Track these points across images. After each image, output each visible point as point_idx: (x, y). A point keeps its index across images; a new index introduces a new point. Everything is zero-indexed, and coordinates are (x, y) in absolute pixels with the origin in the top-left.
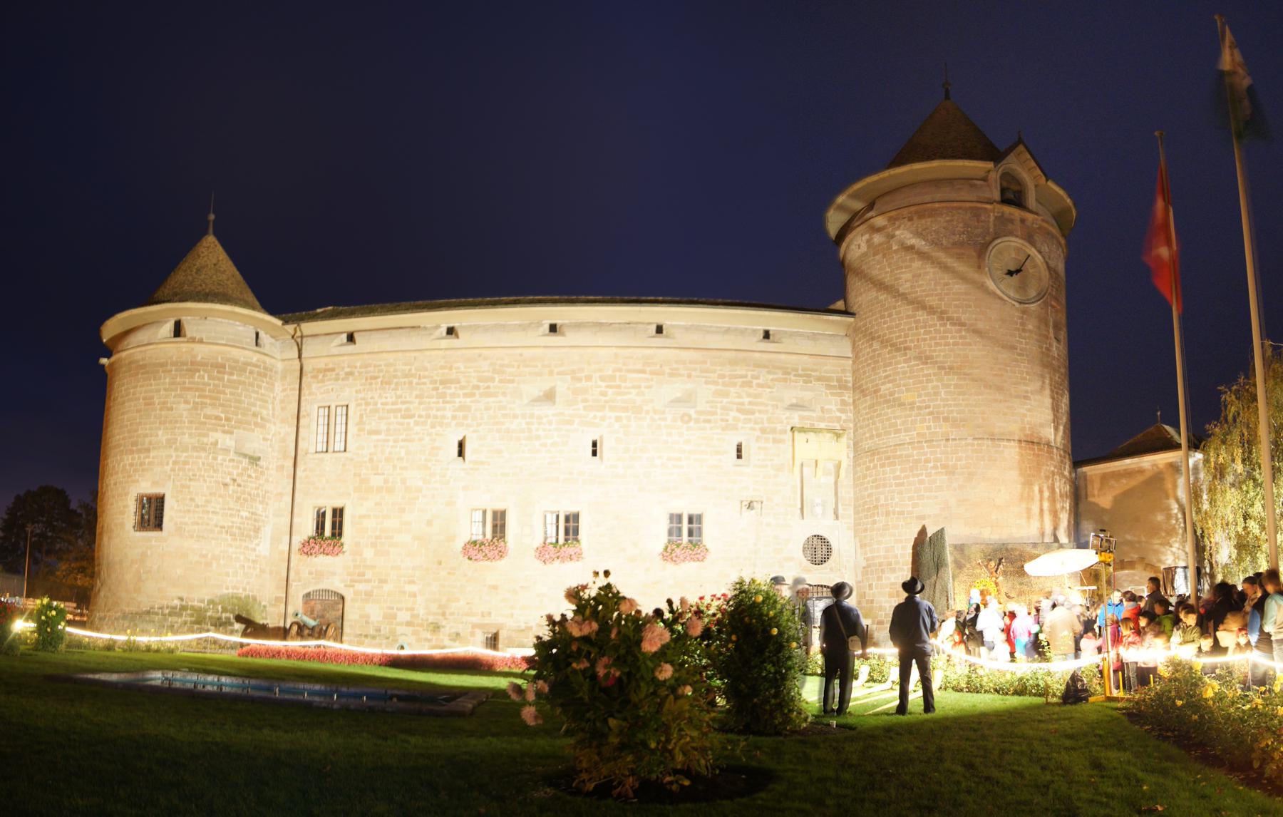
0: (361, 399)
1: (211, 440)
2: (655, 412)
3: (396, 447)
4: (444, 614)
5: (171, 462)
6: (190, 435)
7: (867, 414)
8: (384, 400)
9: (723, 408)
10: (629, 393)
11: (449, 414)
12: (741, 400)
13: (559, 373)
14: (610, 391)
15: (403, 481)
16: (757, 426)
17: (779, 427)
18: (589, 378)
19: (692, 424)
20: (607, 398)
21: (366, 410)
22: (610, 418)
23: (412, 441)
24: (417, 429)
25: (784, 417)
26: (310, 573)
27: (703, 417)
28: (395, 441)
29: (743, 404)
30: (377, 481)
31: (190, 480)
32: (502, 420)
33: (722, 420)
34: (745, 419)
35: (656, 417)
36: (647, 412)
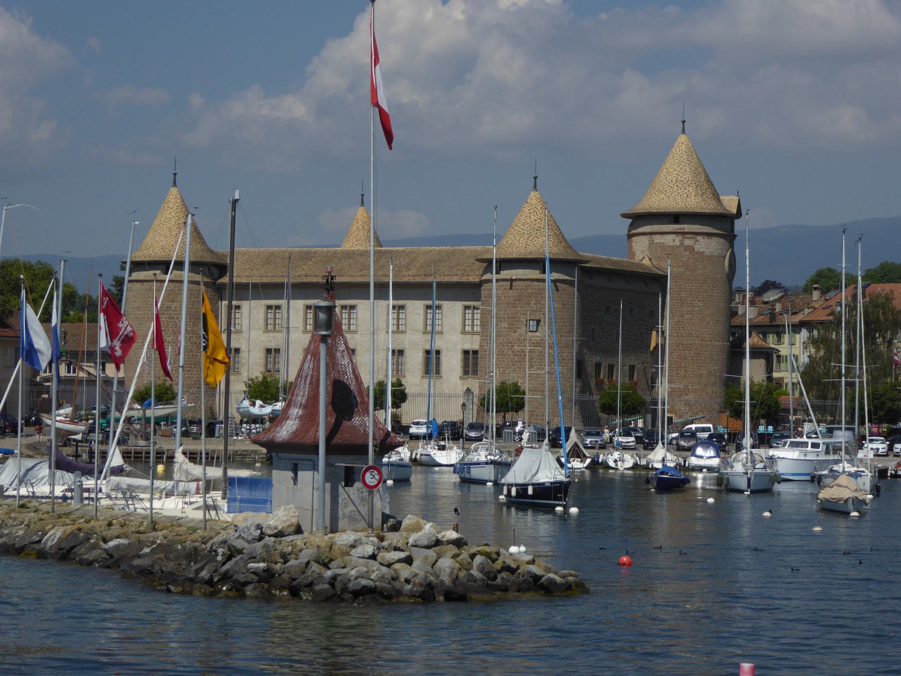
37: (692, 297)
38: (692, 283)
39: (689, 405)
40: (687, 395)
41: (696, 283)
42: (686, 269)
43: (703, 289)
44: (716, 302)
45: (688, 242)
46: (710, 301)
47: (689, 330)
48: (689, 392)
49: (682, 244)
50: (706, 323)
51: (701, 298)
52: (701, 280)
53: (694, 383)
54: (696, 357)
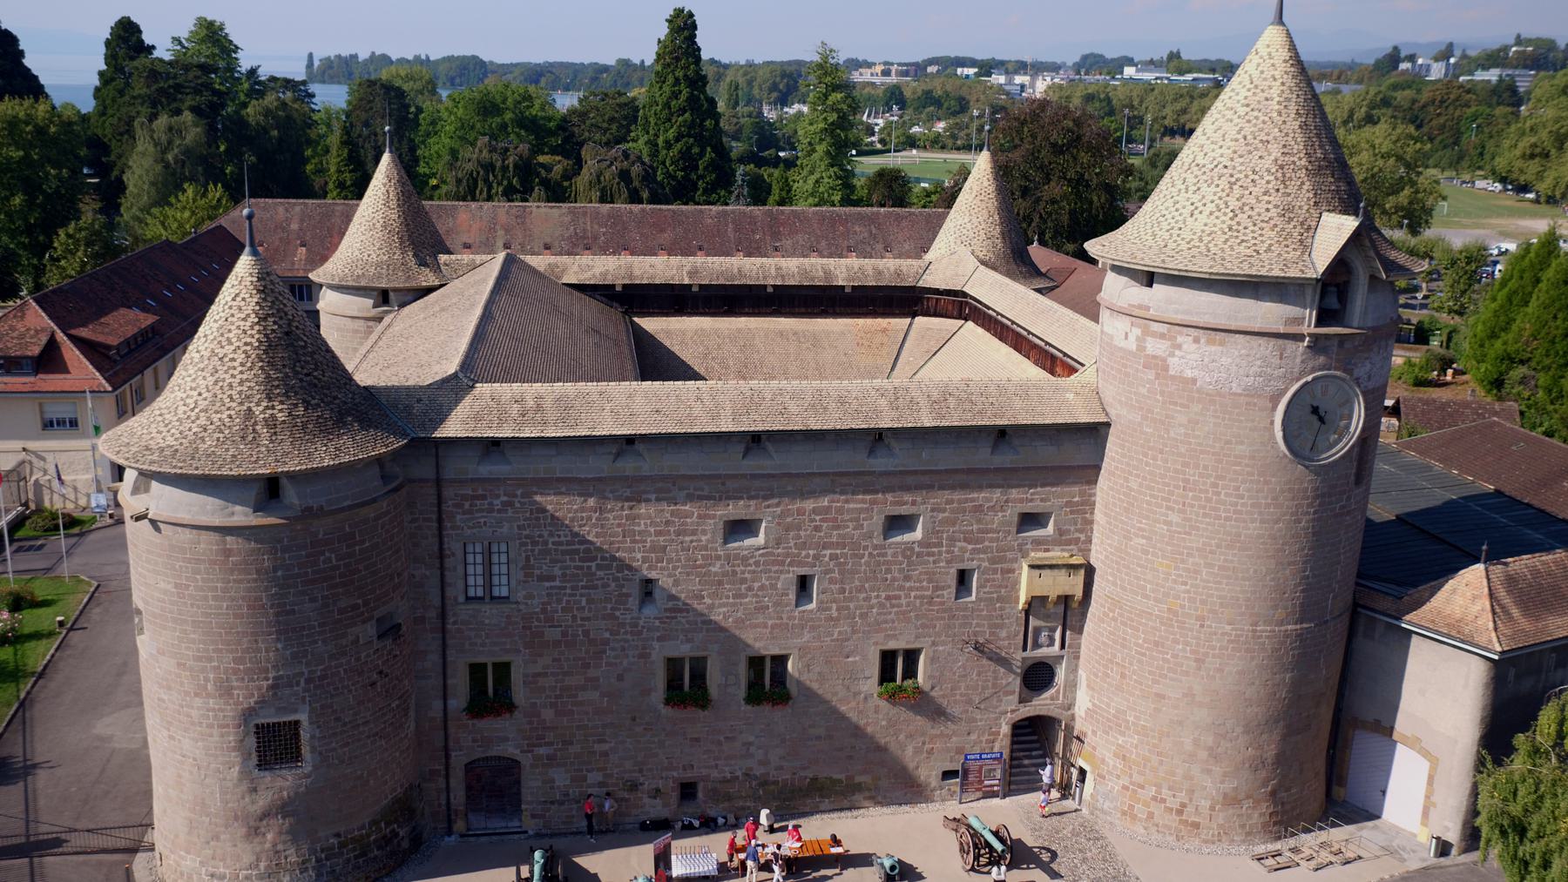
0: (527, 537)
1: (350, 638)
3: (575, 595)
4: (641, 771)
5: (302, 681)
6: (324, 641)
8: (557, 539)
11: (639, 556)
15: (586, 633)
21: (533, 551)
23: (595, 587)
24: (600, 573)
26: (474, 741)
28: (573, 588)
30: (552, 634)
31: (332, 696)
33: (948, 552)
36: (866, 548)
37: (1151, 496)
41: (1166, 461)
43: (1186, 481)
49: (1141, 348)
51: (1176, 502)
54: (1147, 649)
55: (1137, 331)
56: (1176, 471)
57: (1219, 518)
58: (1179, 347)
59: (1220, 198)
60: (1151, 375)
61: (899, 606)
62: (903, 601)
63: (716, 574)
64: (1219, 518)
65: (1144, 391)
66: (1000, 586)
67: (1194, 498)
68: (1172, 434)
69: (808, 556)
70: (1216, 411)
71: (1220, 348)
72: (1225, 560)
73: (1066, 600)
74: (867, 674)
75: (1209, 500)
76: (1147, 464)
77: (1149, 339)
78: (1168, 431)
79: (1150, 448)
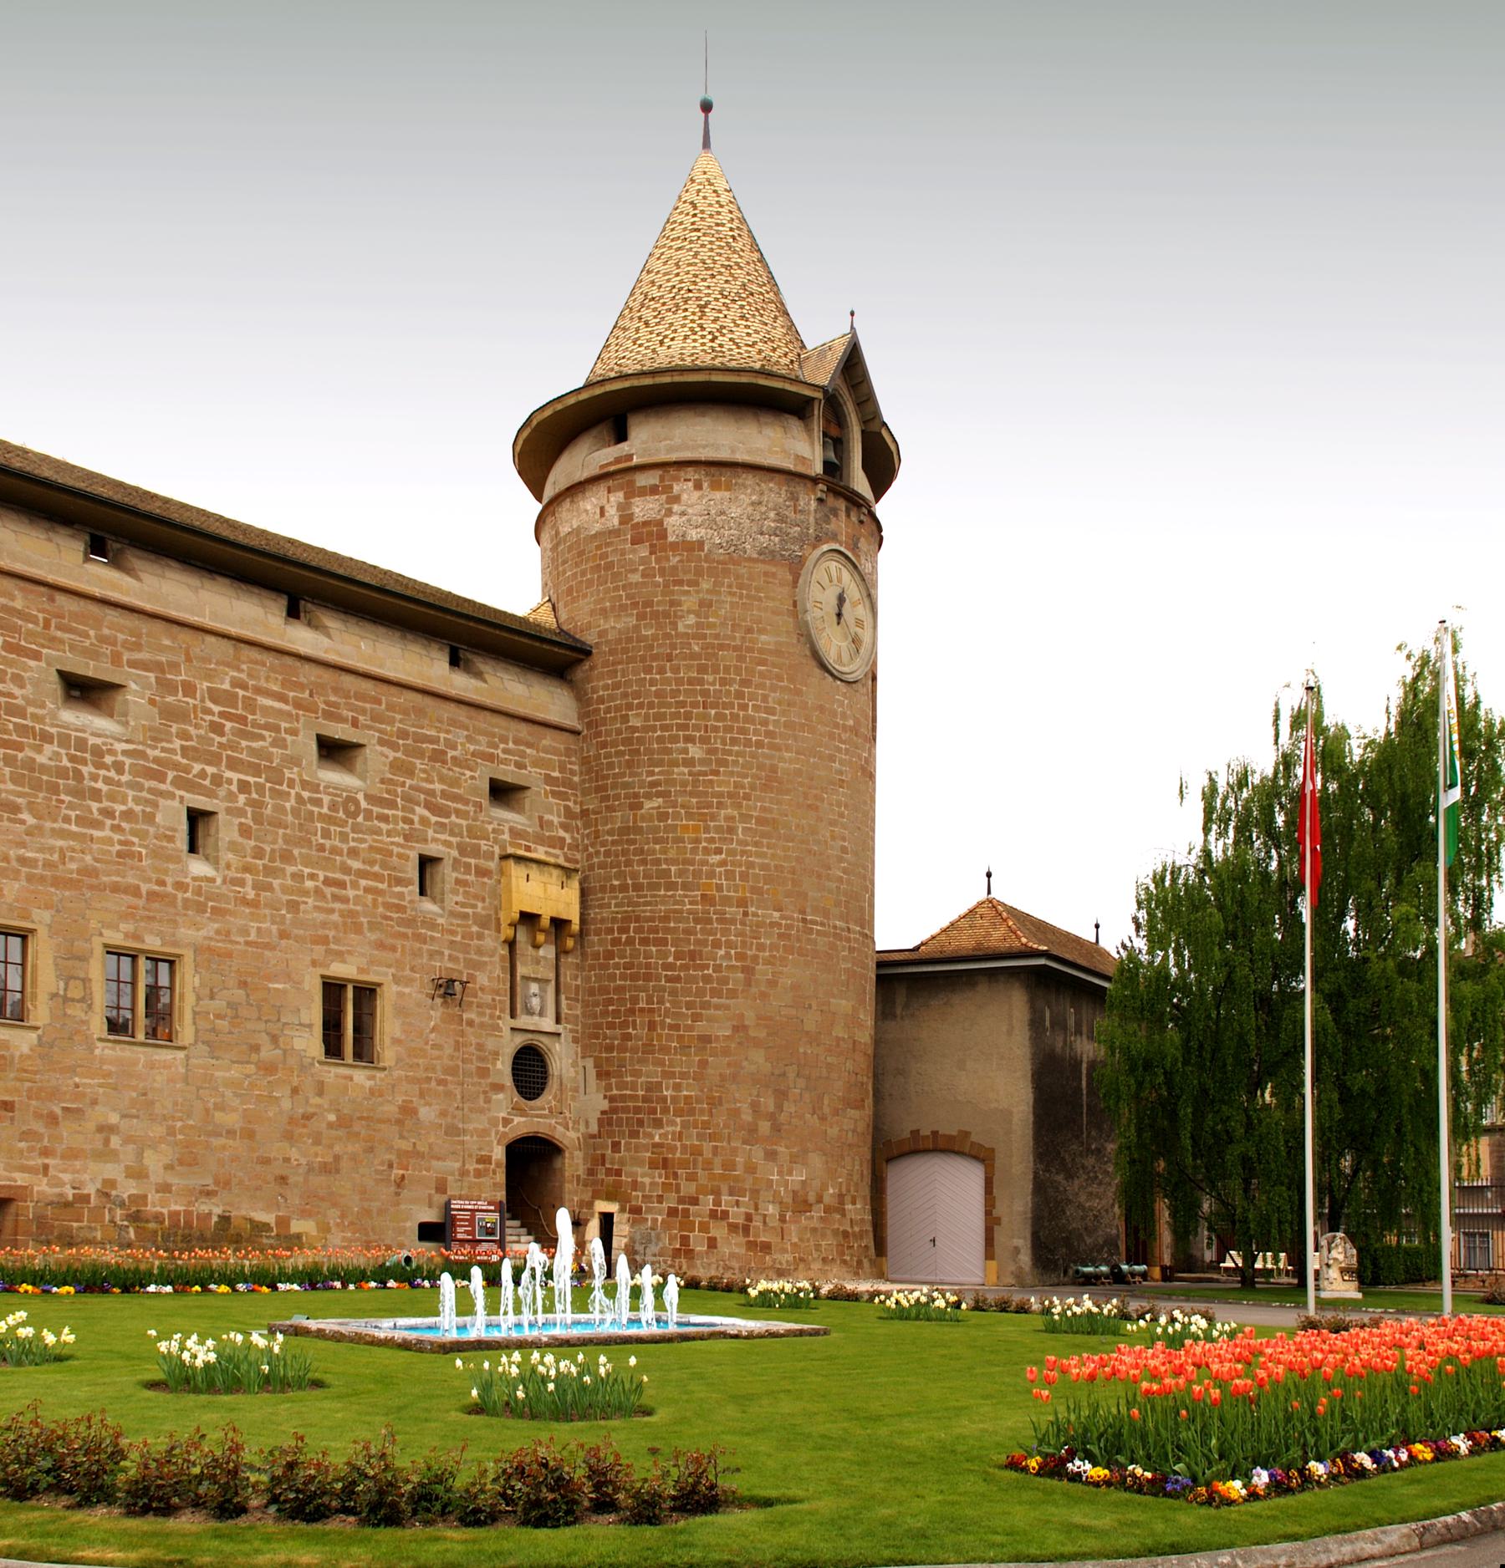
2: (305, 785)
7: (614, 843)
9: (407, 798)
10: (263, 738)
12: (431, 786)
13: (133, 664)
14: (228, 725)
16: (454, 840)
17: (484, 845)
18: (189, 689)
19: (360, 819)
20: (224, 740)
22: (230, 781)
25: (490, 828)
27: (376, 810)
29: (431, 793)
32: (14, 737)
33: (406, 820)
34: (437, 823)
35: (306, 794)
38: (661, 671)
39: (665, 1163)
40: (658, 1124)
42: (641, 617)
44: (759, 744)
45: (644, 509)
46: (734, 741)
47: (657, 862)
48: (665, 1110)
50: (718, 829)
52: (694, 656)
53: (683, 1075)
55: (618, 497)
56: (691, 682)
57: (748, 743)
58: (676, 499)
59: (693, 321)
60: (643, 550)
61: (346, 900)
62: (351, 893)
63: (43, 769)
64: (748, 743)
65: (636, 578)
66: (476, 897)
67: (720, 717)
68: (681, 629)
69: (203, 774)
70: (730, 586)
71: (727, 494)
72: (764, 809)
73: (559, 924)
74: (305, 1019)
75: (735, 717)
76: (653, 682)
77: (636, 500)
78: (674, 625)
79: (655, 658)
